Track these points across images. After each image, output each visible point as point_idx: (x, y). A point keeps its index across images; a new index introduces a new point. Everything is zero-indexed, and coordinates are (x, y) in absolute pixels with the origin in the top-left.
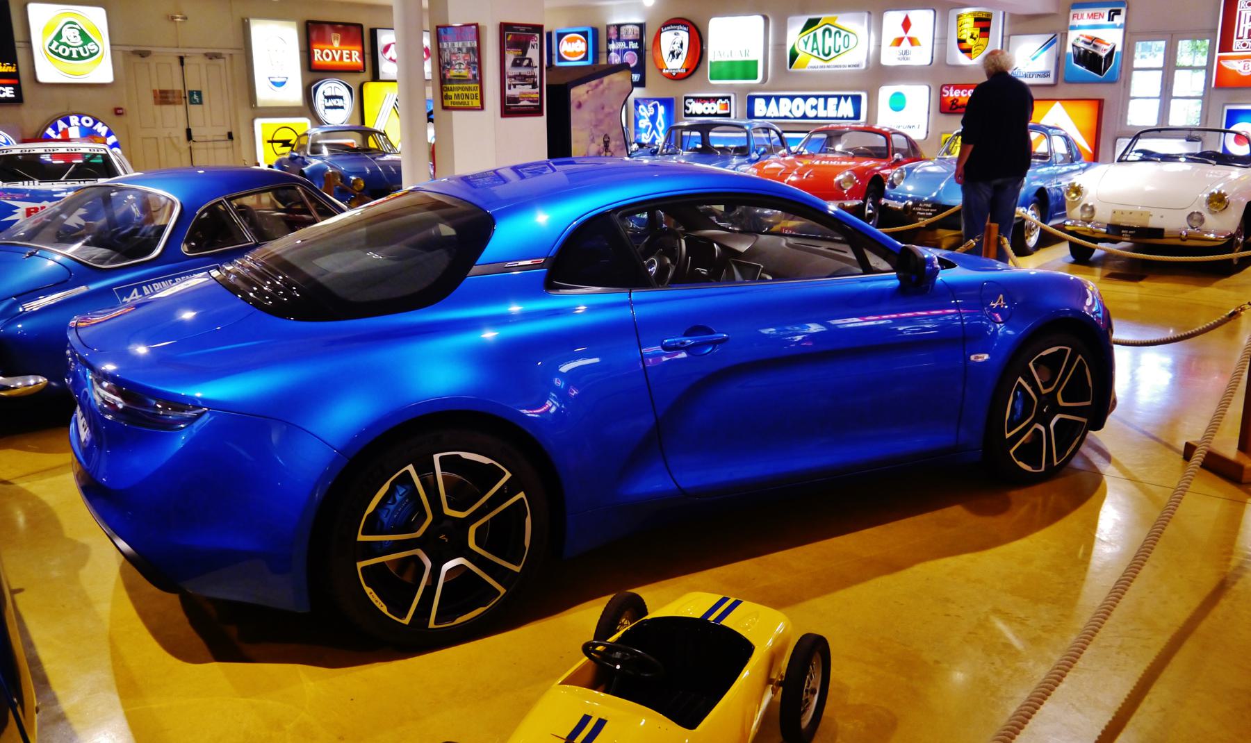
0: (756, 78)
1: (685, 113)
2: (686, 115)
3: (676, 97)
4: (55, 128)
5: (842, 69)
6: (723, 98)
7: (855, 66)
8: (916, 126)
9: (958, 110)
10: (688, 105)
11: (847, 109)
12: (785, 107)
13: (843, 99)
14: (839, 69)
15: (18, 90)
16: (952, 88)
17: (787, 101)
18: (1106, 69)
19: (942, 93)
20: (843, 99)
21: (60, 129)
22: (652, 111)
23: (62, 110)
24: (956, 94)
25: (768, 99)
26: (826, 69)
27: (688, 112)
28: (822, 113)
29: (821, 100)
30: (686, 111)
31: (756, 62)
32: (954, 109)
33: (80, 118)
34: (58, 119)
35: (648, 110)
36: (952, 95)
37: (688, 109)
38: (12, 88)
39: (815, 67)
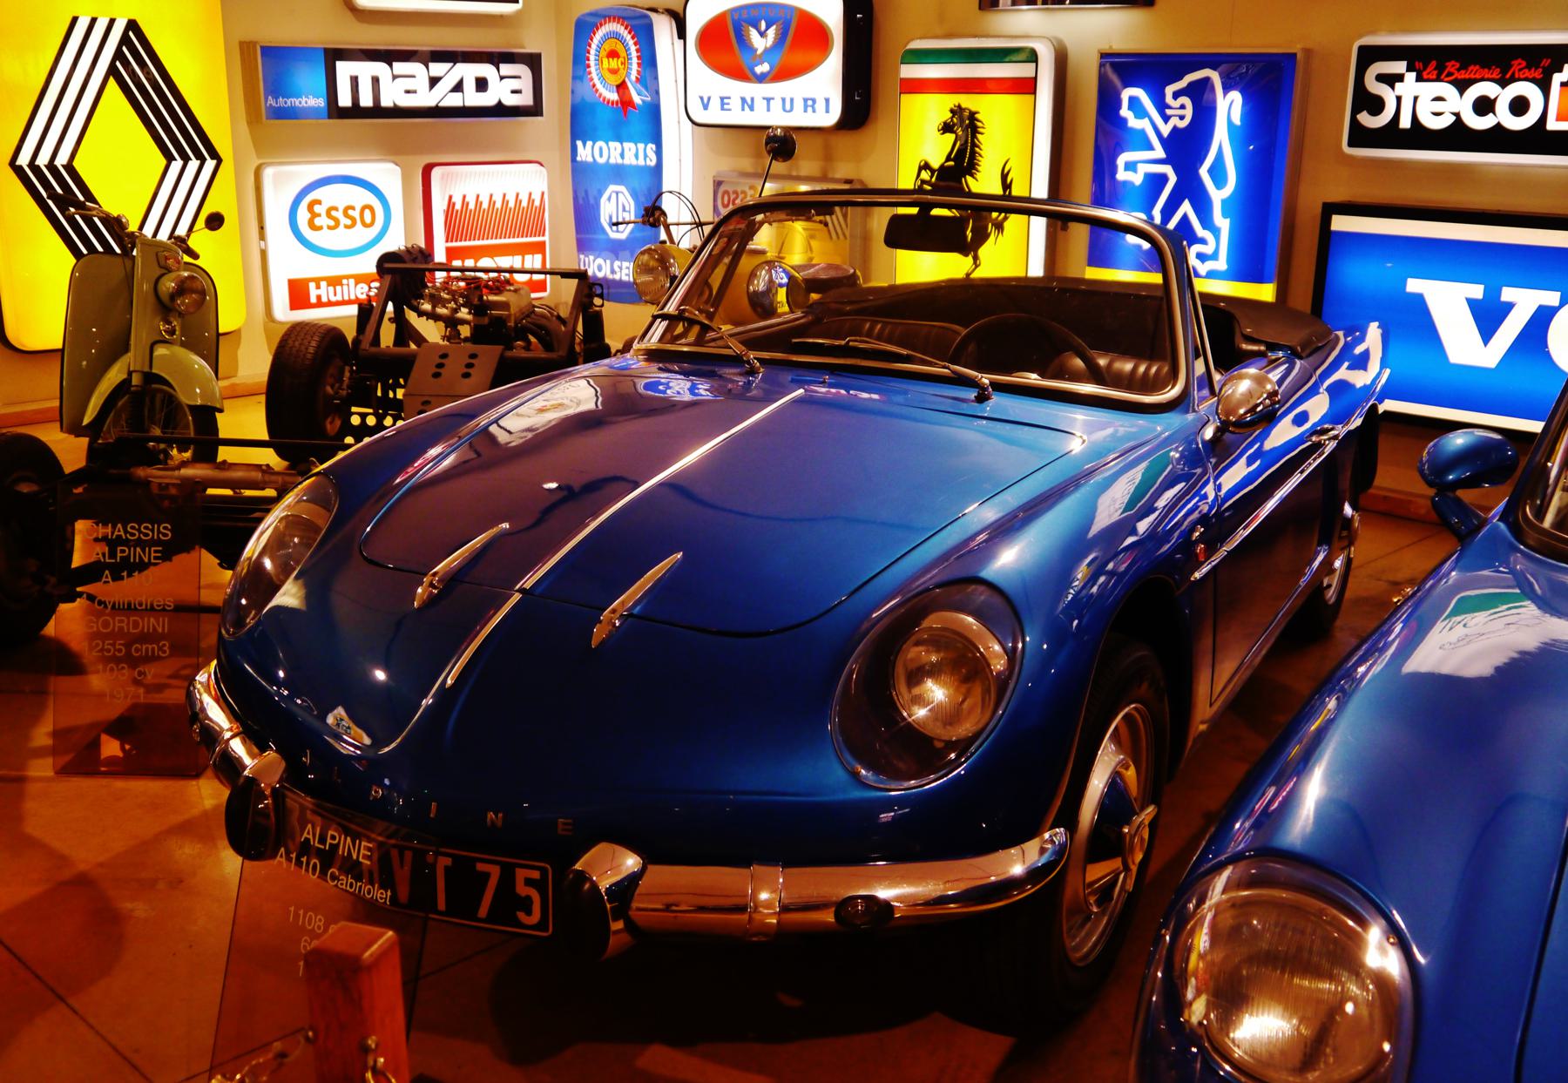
2: (1361, 136)
3: (1308, 52)
10: (1382, 90)
22: (1182, 113)
30: (1365, 119)
35: (1162, 107)
37: (1376, 105)
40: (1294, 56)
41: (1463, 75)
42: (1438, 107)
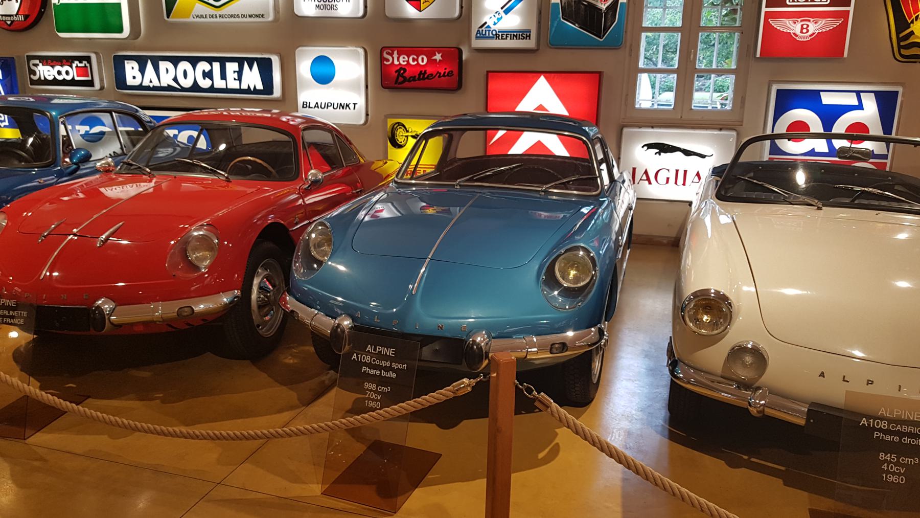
0: (120, 30)
1: (30, 78)
2: (33, 82)
5: (241, 20)
6: (81, 59)
7: (257, 16)
8: (352, 106)
9: (406, 84)
11: (252, 78)
12: (167, 74)
13: (246, 66)
14: (237, 20)
16: (395, 52)
17: (170, 65)
18: (606, 29)
19: (383, 59)
20: (246, 66)
24: (403, 60)
25: (142, 63)
26: (219, 20)
27: (35, 78)
28: (219, 83)
29: (216, 66)
30: (32, 76)
31: (118, 5)
32: (400, 83)
36: (396, 62)
37: (34, 73)
39: (202, 16)
40: (13, 58)
41: (51, 64)
42: (49, 73)
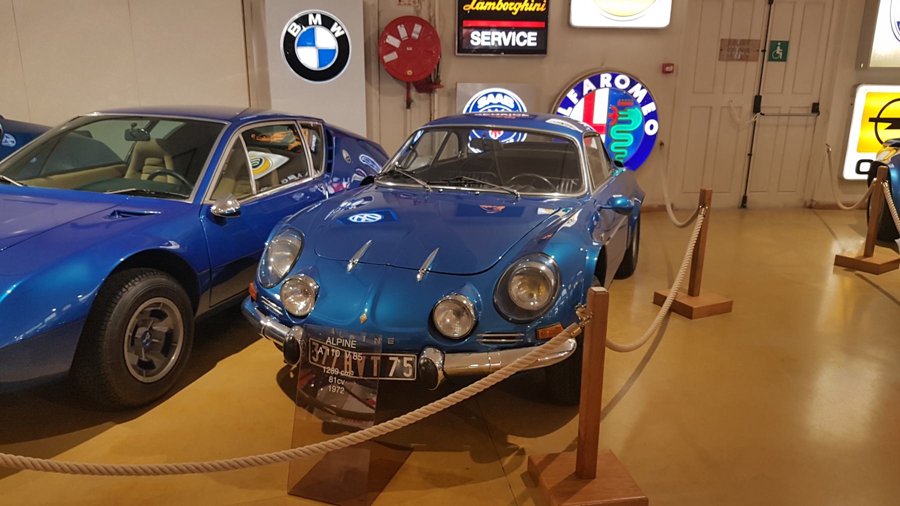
4: (579, 89)
15: (543, 38)
21: (585, 92)
23: (592, 66)
33: (614, 76)
34: (584, 78)
38: (535, 34)
